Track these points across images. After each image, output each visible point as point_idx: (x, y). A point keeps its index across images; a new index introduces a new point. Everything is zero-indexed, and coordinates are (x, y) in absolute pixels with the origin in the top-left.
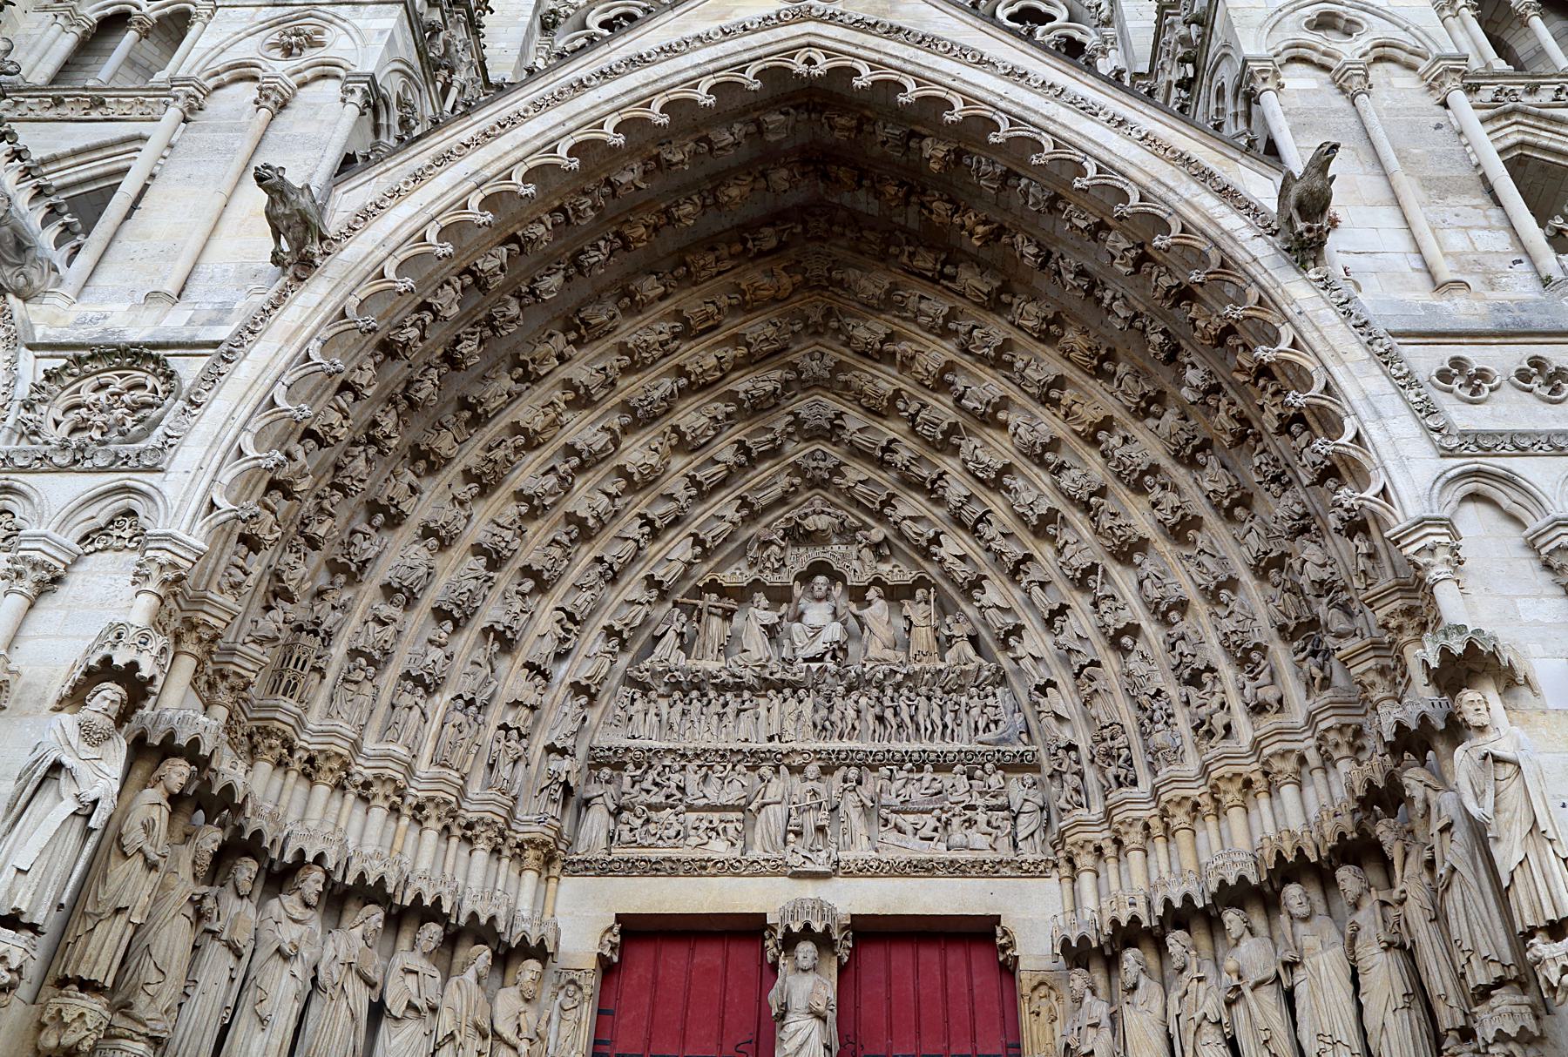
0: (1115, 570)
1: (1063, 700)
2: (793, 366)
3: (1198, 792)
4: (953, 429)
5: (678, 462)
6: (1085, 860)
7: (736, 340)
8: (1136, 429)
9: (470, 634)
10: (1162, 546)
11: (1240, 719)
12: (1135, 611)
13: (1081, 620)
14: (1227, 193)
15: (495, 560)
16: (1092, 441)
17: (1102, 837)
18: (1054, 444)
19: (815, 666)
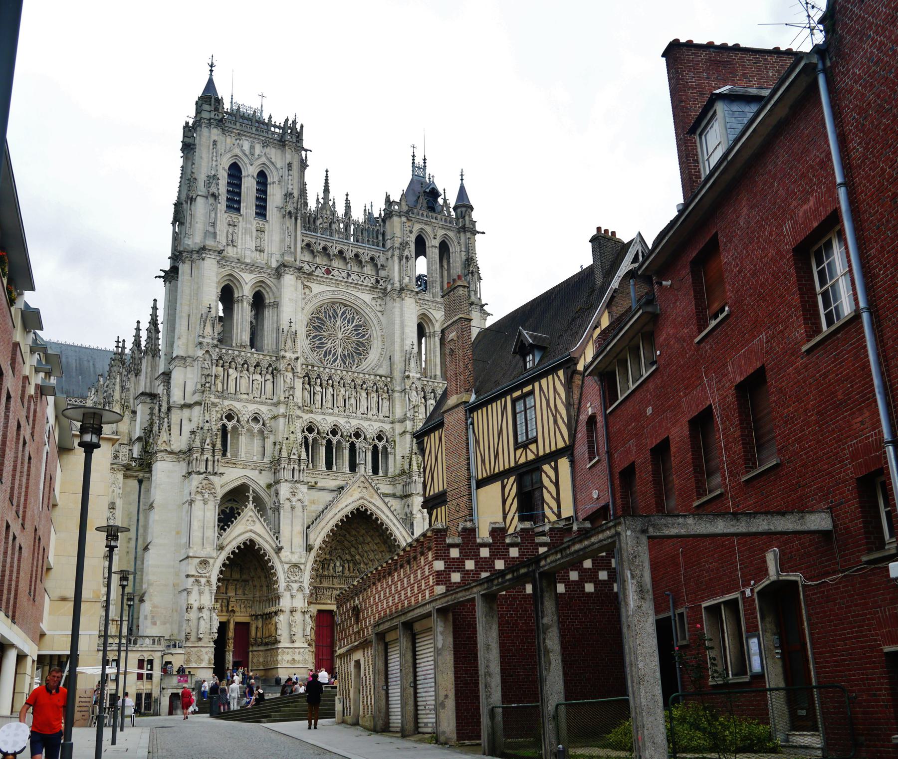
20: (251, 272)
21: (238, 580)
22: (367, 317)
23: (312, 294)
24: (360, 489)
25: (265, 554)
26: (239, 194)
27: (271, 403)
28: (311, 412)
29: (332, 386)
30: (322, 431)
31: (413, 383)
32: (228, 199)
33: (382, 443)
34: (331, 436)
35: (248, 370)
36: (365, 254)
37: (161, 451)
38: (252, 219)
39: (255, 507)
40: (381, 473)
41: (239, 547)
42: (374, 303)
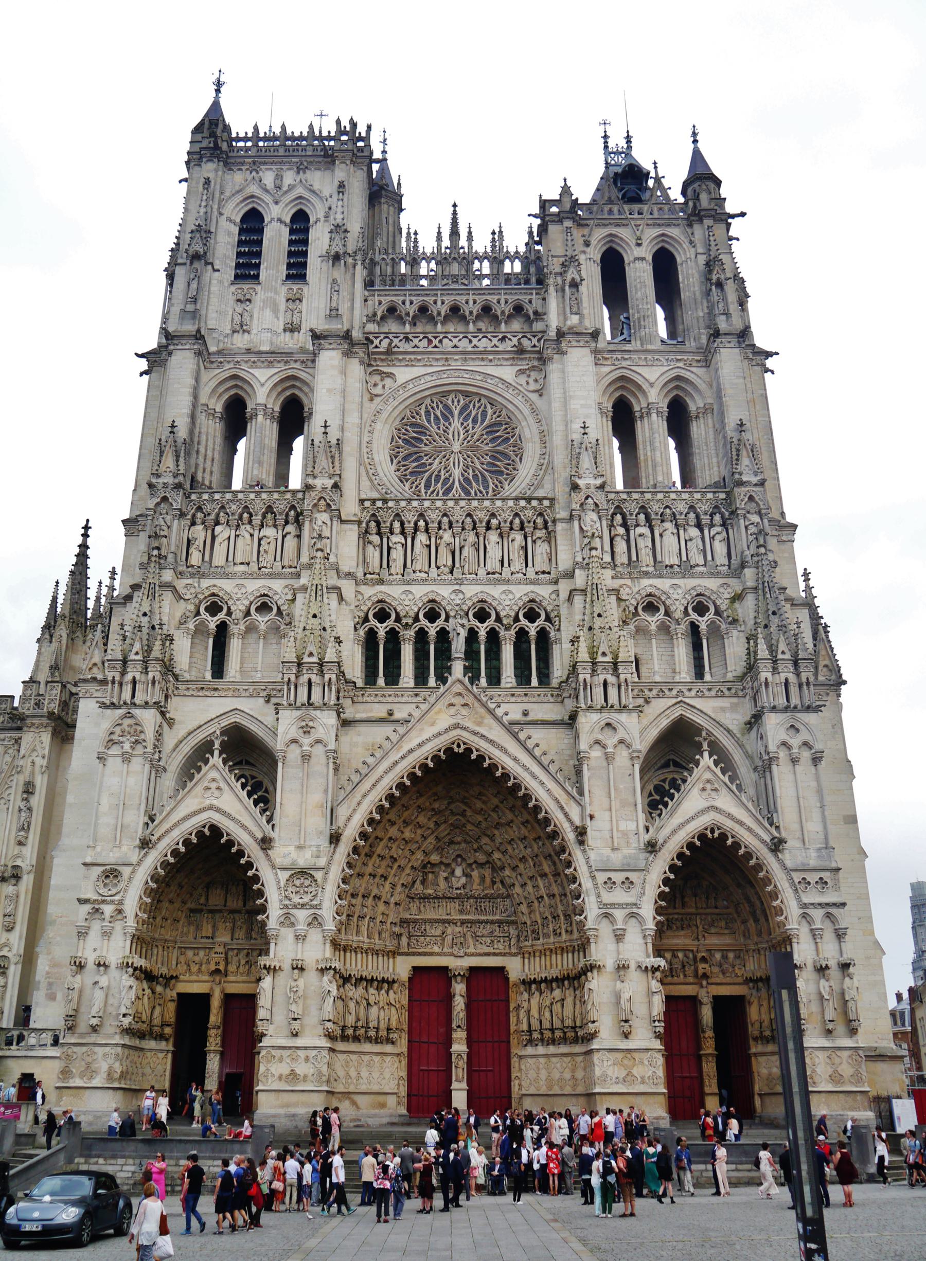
0: (539, 878)
1: (524, 908)
2: (451, 797)
3: (552, 947)
4: (498, 823)
5: (419, 831)
6: (526, 956)
7: (435, 794)
8: (546, 841)
9: (371, 898)
10: (550, 877)
11: (563, 931)
12: (543, 892)
13: (529, 888)
14: (566, 815)
15: (374, 876)
16: (535, 840)
17: (530, 950)
18: (525, 838)
19: (459, 892)
20: (270, 364)
21: (239, 912)
22: (510, 406)
23: (396, 385)
24: (452, 710)
25: (241, 853)
26: (258, 254)
27: (292, 573)
28: (381, 582)
29: (427, 530)
30: (402, 614)
31: (587, 498)
32: (238, 266)
33: (536, 624)
34: (424, 622)
35: (250, 522)
36: (503, 302)
37: (85, 681)
38: (279, 282)
39: (225, 762)
40: (534, 682)
41: (187, 842)
42: (522, 379)
